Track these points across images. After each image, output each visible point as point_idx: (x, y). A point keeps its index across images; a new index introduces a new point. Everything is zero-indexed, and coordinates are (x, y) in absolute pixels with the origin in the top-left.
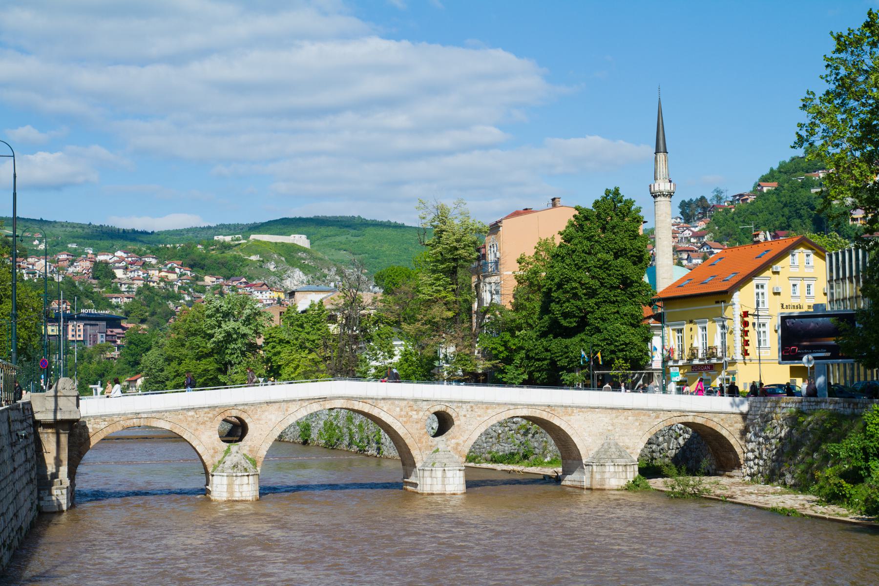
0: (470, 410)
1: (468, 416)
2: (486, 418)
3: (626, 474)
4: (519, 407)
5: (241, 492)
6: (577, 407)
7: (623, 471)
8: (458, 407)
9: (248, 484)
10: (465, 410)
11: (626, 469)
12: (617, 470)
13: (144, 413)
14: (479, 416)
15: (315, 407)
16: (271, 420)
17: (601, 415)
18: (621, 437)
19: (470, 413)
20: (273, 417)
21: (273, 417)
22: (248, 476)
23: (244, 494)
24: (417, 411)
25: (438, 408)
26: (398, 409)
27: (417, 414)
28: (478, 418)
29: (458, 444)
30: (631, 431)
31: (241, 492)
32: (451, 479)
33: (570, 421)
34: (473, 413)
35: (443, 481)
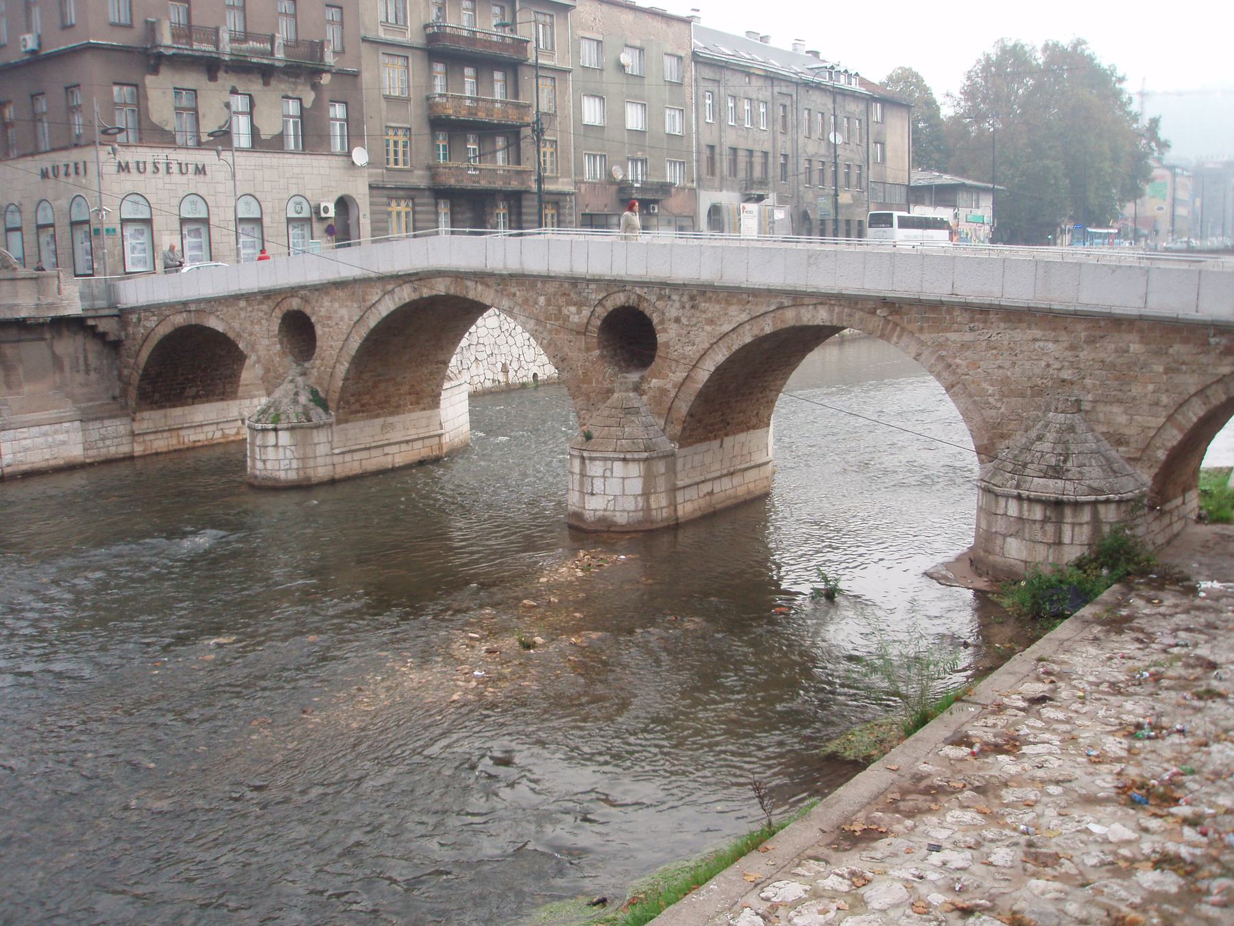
0: (687, 306)
1: (684, 321)
2: (727, 328)
3: (1059, 533)
4: (806, 301)
5: (264, 461)
6: (967, 307)
7: (1045, 520)
8: (660, 298)
9: (276, 446)
10: (677, 305)
12: (1026, 515)
13: (193, 301)
14: (711, 322)
15: (406, 294)
16: (342, 319)
17: (1038, 333)
18: (1101, 407)
19: (688, 312)
21: (344, 312)
22: (276, 430)
23: (269, 465)
24: (580, 305)
25: (620, 299)
26: (542, 300)
27: (579, 312)
28: (708, 328)
30: (1136, 390)
31: (264, 461)
32: (598, 484)
34: (698, 314)
35: (582, 484)
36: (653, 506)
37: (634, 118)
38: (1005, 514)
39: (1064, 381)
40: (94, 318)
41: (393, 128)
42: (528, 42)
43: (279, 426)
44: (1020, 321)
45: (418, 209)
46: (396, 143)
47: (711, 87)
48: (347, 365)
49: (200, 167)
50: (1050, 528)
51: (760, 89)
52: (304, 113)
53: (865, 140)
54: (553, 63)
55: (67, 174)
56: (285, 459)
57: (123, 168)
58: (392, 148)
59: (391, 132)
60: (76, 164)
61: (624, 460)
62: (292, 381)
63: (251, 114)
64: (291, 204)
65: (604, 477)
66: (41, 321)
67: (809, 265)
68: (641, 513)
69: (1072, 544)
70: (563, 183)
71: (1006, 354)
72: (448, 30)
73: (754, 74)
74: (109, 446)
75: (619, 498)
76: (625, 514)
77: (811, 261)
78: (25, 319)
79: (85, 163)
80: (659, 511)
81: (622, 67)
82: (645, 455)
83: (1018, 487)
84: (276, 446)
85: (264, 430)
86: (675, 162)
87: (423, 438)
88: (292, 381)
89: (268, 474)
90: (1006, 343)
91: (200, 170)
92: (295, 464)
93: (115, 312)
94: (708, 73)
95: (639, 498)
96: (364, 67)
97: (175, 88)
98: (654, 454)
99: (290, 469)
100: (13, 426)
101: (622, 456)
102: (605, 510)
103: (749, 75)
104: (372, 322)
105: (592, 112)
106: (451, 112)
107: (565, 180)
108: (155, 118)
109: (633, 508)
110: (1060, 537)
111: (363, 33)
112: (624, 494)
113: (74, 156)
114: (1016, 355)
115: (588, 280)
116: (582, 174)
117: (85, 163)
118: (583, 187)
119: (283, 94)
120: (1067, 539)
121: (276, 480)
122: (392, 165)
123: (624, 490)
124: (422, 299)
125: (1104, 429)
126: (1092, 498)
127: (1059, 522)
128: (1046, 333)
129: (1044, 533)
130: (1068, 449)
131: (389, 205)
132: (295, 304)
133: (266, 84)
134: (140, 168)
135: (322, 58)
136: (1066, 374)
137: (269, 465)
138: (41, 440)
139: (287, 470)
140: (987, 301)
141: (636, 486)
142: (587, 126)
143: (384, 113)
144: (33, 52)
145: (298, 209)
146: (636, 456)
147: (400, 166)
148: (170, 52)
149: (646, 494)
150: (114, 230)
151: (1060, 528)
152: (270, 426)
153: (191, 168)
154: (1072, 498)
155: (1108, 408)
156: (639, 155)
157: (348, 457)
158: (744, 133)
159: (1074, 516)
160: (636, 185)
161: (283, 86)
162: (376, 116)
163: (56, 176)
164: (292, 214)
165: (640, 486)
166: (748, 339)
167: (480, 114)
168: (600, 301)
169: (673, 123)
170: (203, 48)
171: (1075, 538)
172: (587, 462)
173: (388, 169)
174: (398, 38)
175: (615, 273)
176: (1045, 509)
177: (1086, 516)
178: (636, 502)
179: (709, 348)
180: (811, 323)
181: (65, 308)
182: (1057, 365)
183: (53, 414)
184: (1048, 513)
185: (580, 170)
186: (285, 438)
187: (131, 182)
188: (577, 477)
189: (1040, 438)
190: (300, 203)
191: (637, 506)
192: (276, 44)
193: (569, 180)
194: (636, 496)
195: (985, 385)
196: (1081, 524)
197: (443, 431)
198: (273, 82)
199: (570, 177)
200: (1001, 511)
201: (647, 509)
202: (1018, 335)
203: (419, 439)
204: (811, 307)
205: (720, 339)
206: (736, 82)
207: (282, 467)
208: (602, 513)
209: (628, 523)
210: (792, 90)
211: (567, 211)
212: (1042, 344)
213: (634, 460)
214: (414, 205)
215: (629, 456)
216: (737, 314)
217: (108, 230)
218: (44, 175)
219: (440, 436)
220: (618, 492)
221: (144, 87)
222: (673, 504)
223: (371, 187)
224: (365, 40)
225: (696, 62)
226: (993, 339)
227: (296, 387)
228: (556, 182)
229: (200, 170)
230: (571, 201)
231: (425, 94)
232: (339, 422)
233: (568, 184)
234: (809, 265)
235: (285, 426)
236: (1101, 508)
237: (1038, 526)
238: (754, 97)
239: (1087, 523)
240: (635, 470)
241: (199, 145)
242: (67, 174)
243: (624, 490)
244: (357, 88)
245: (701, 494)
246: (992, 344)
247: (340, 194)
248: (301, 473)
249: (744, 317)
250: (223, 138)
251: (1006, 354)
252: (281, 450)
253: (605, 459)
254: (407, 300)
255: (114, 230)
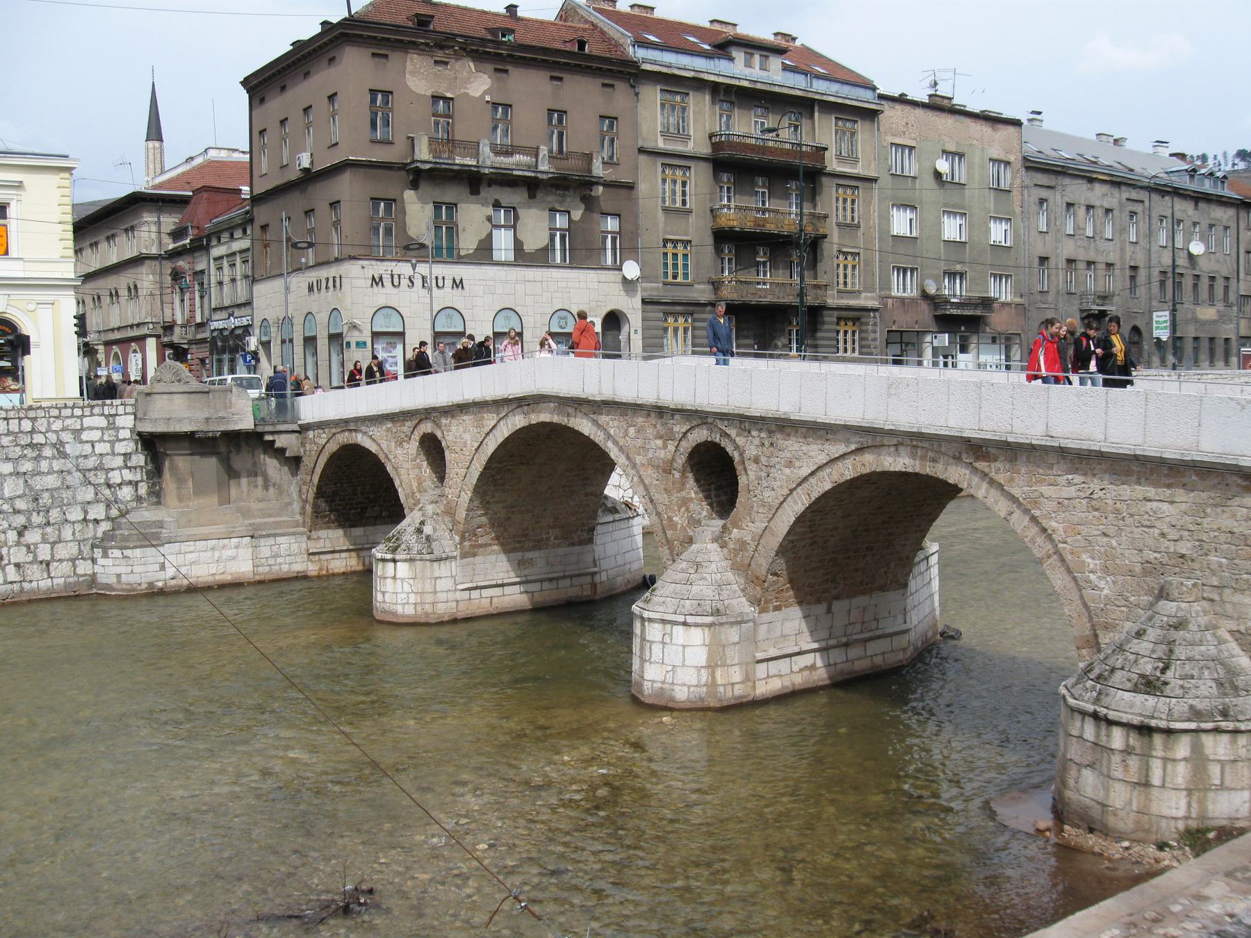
1: (763, 459)
2: (805, 471)
3: (1147, 770)
5: (384, 593)
7: (1128, 751)
9: (394, 578)
10: (757, 441)
11: (1151, 747)
14: (790, 464)
15: (518, 421)
17: (1151, 492)
20: (467, 437)
22: (394, 561)
28: (787, 471)
29: (743, 544)
31: (384, 593)
32: (657, 649)
33: (1036, 503)
36: (719, 682)
37: (951, 229)
38: (1080, 737)
39: (1182, 556)
40: (273, 433)
41: (672, 241)
42: (826, 149)
43: (397, 557)
44: (1129, 473)
45: (698, 324)
46: (675, 255)
47: (1044, 193)
48: (470, 494)
49: (458, 282)
50: (1133, 762)
51: (1104, 195)
52: (573, 226)
53: (1235, 250)
54: (856, 171)
55: (327, 288)
56: (403, 592)
57: (377, 281)
58: (670, 261)
59: (669, 245)
60: (334, 278)
61: (685, 624)
62: (420, 509)
63: (514, 227)
64: (555, 320)
65: (663, 643)
66: (210, 434)
67: (890, 395)
68: (704, 689)
69: (1163, 786)
70: (866, 298)
71: (1111, 516)
72: (735, 139)
73: (1096, 179)
74: (280, 564)
75: (679, 670)
76: (685, 689)
77: (892, 391)
78: (193, 433)
79: (341, 277)
80: (729, 688)
81: (938, 175)
82: (709, 620)
83: (1097, 701)
84: (394, 578)
85: (384, 560)
86: (1001, 276)
87: (571, 577)
88: (420, 509)
89: (386, 606)
90: (1110, 502)
91: (458, 284)
92: (412, 599)
93: (295, 427)
94: (1042, 179)
95: (703, 671)
96: (640, 178)
97: (372, 199)
98: (724, 619)
99: (408, 603)
100: (178, 539)
101: (681, 619)
102: (663, 682)
103: (1091, 180)
104: (491, 446)
105: (901, 223)
106: (735, 223)
107: (869, 295)
108: (412, 232)
109: (695, 682)
110: (1147, 776)
111: (640, 143)
112: (684, 665)
113: (332, 271)
114: (1123, 519)
115: (673, 410)
116: (889, 289)
117: (341, 277)
118: (890, 301)
119: (551, 206)
120: (1156, 780)
121: (394, 614)
122: (670, 279)
123: (684, 660)
124: (531, 426)
125: (1233, 625)
126: (1193, 726)
127: (1146, 756)
128: (1160, 490)
129: (1126, 768)
130: (1171, 651)
131: (666, 320)
132: (427, 427)
133: (532, 196)
134: (395, 282)
135: (590, 171)
136: (1185, 548)
137: (388, 598)
138: (209, 554)
139: (404, 604)
140: (1085, 445)
141: (699, 656)
142: (896, 238)
143: (661, 226)
144: (306, 170)
145: (563, 323)
146: (699, 620)
147: (680, 279)
148: (428, 166)
149: (711, 666)
150: (365, 343)
151: (1147, 763)
152: (389, 556)
153: (449, 283)
154: (1163, 724)
155: (1238, 598)
156: (958, 268)
157: (475, 594)
158: (1085, 243)
159: (1166, 748)
160: (953, 300)
161: (550, 198)
162: (655, 226)
163: (319, 290)
164: (555, 329)
165: (704, 657)
166: (828, 486)
167: (768, 225)
168: (685, 433)
169: (998, 233)
170: (466, 163)
171: (1168, 779)
172: (646, 623)
173: (665, 284)
174: (678, 148)
175: (698, 401)
176: (1128, 736)
177: (1182, 748)
178: (699, 675)
179: (788, 495)
180: (892, 469)
181: (236, 423)
182: (1173, 534)
183: (220, 529)
184: (1131, 741)
185: (886, 285)
186: (403, 569)
187: (385, 295)
188: (638, 640)
189: (1139, 634)
190: (565, 318)
191: (699, 680)
192: (541, 156)
193: (874, 294)
194: (699, 668)
195: (1085, 557)
196: (1174, 760)
197: (596, 569)
198: (539, 195)
199: (874, 291)
200: (1074, 733)
201: (713, 684)
202: (1126, 491)
203: (564, 577)
204: (892, 449)
205: (799, 484)
206: (1077, 191)
207: (399, 601)
208: (659, 685)
209: (688, 700)
210: (1143, 195)
211: (870, 328)
212: (1155, 504)
213: (696, 625)
214: (694, 320)
215: (690, 619)
216: (817, 452)
217: (358, 344)
218: (311, 289)
219: (593, 574)
220: (678, 663)
221: (403, 202)
222: (748, 679)
223: (644, 302)
224: (642, 151)
225: (1027, 168)
226: (1095, 496)
227: (423, 515)
228: (858, 298)
229: (458, 284)
230: (875, 317)
231: (708, 205)
232: (464, 555)
233: (872, 298)
234: (890, 395)
235: (404, 557)
236: (1208, 741)
237: (1116, 759)
238: (1097, 203)
239: (1185, 759)
240: (697, 636)
241: (461, 260)
242: (327, 288)
243: (684, 660)
244: (634, 201)
245: (796, 668)
246: (1094, 503)
247: (609, 309)
248: (419, 608)
249: (823, 458)
250: (484, 253)
251: (1111, 516)
252: (399, 582)
253: (663, 622)
254: (518, 427)
255: (365, 343)
